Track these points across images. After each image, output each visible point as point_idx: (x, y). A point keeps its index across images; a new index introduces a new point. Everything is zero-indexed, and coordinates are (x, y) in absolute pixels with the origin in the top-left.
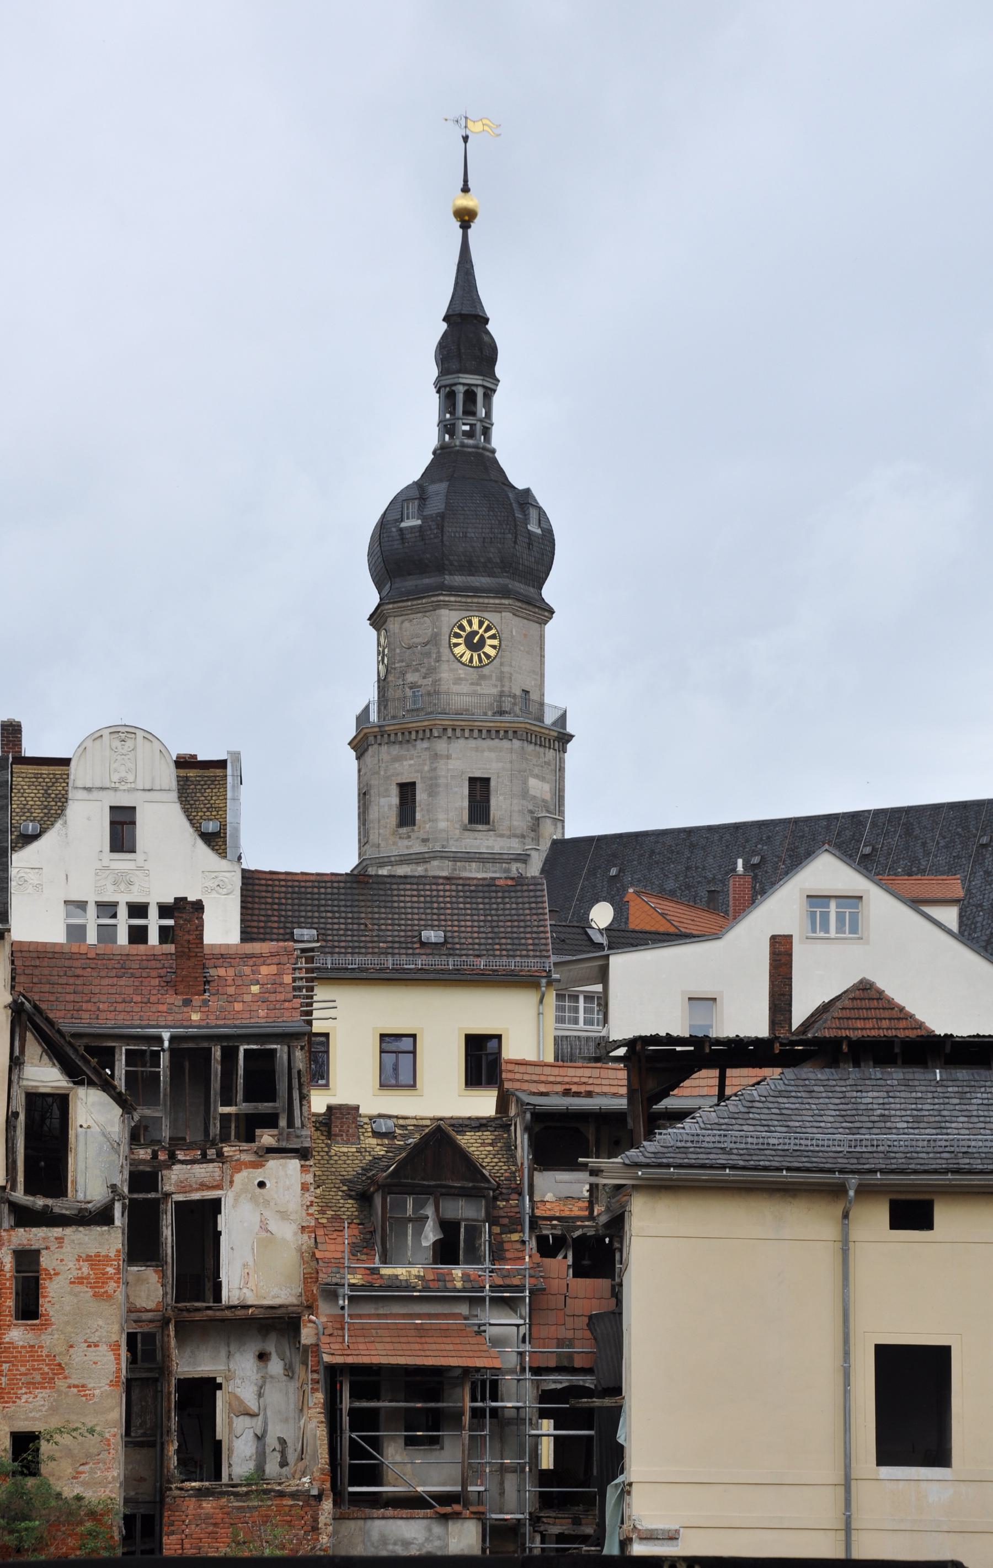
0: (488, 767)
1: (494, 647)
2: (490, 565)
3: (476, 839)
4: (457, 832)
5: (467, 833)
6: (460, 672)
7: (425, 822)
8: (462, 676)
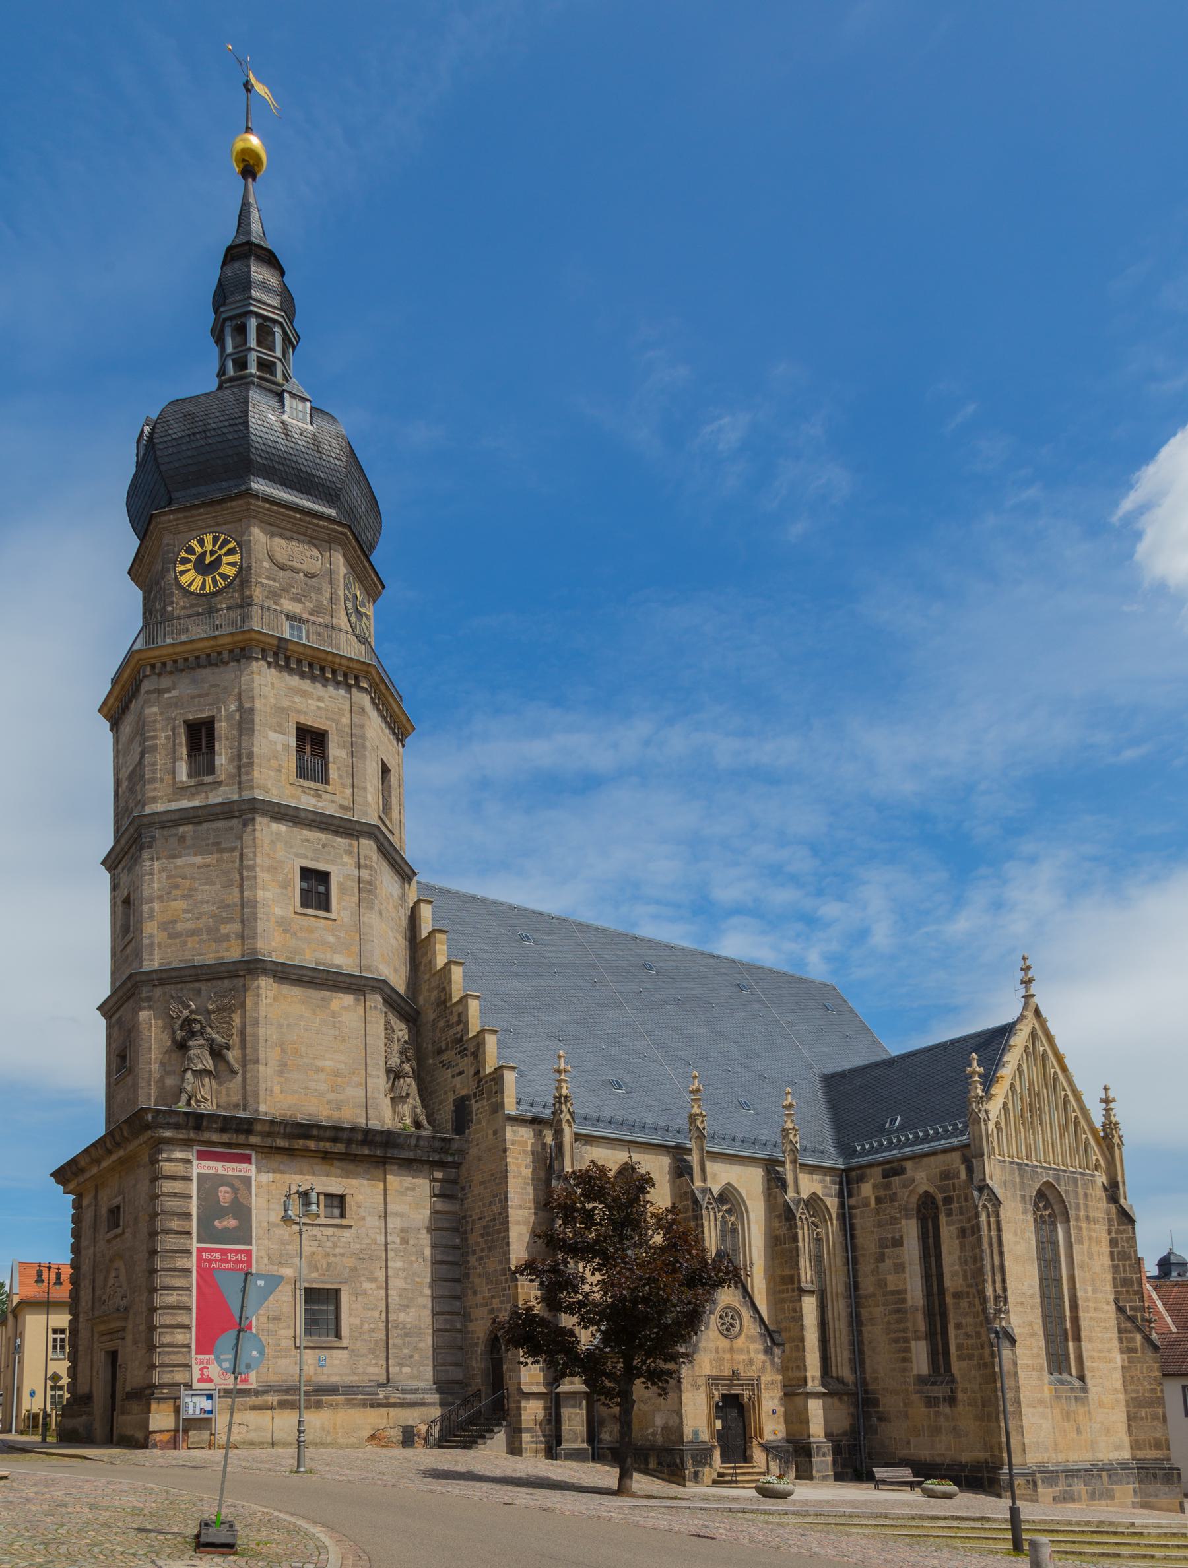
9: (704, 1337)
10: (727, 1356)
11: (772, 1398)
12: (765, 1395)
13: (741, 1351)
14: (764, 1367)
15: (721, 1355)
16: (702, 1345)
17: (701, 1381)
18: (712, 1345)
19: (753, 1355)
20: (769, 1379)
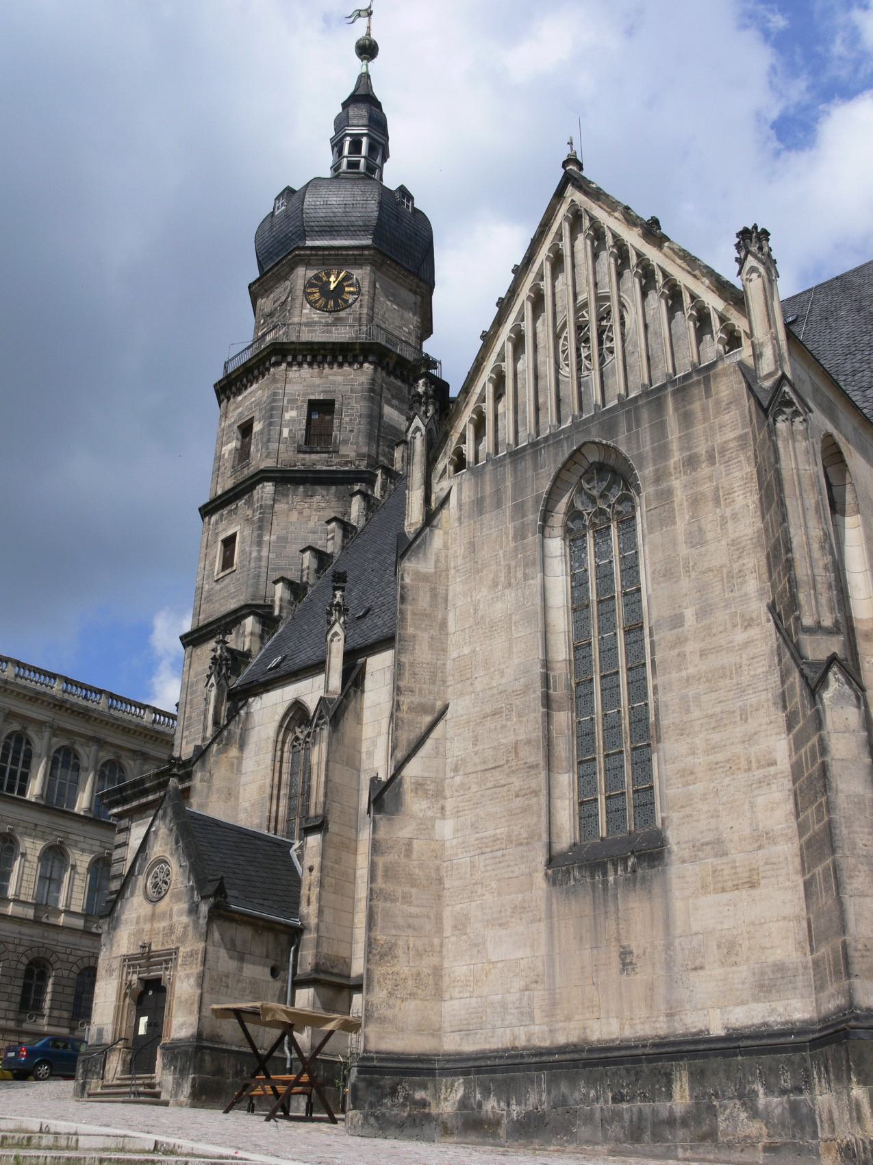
9: (128, 906)
10: (147, 927)
11: (188, 976)
12: (181, 972)
13: (163, 916)
14: (185, 934)
15: (142, 925)
16: (124, 917)
17: (116, 964)
18: (134, 915)
19: (175, 919)
20: (188, 949)
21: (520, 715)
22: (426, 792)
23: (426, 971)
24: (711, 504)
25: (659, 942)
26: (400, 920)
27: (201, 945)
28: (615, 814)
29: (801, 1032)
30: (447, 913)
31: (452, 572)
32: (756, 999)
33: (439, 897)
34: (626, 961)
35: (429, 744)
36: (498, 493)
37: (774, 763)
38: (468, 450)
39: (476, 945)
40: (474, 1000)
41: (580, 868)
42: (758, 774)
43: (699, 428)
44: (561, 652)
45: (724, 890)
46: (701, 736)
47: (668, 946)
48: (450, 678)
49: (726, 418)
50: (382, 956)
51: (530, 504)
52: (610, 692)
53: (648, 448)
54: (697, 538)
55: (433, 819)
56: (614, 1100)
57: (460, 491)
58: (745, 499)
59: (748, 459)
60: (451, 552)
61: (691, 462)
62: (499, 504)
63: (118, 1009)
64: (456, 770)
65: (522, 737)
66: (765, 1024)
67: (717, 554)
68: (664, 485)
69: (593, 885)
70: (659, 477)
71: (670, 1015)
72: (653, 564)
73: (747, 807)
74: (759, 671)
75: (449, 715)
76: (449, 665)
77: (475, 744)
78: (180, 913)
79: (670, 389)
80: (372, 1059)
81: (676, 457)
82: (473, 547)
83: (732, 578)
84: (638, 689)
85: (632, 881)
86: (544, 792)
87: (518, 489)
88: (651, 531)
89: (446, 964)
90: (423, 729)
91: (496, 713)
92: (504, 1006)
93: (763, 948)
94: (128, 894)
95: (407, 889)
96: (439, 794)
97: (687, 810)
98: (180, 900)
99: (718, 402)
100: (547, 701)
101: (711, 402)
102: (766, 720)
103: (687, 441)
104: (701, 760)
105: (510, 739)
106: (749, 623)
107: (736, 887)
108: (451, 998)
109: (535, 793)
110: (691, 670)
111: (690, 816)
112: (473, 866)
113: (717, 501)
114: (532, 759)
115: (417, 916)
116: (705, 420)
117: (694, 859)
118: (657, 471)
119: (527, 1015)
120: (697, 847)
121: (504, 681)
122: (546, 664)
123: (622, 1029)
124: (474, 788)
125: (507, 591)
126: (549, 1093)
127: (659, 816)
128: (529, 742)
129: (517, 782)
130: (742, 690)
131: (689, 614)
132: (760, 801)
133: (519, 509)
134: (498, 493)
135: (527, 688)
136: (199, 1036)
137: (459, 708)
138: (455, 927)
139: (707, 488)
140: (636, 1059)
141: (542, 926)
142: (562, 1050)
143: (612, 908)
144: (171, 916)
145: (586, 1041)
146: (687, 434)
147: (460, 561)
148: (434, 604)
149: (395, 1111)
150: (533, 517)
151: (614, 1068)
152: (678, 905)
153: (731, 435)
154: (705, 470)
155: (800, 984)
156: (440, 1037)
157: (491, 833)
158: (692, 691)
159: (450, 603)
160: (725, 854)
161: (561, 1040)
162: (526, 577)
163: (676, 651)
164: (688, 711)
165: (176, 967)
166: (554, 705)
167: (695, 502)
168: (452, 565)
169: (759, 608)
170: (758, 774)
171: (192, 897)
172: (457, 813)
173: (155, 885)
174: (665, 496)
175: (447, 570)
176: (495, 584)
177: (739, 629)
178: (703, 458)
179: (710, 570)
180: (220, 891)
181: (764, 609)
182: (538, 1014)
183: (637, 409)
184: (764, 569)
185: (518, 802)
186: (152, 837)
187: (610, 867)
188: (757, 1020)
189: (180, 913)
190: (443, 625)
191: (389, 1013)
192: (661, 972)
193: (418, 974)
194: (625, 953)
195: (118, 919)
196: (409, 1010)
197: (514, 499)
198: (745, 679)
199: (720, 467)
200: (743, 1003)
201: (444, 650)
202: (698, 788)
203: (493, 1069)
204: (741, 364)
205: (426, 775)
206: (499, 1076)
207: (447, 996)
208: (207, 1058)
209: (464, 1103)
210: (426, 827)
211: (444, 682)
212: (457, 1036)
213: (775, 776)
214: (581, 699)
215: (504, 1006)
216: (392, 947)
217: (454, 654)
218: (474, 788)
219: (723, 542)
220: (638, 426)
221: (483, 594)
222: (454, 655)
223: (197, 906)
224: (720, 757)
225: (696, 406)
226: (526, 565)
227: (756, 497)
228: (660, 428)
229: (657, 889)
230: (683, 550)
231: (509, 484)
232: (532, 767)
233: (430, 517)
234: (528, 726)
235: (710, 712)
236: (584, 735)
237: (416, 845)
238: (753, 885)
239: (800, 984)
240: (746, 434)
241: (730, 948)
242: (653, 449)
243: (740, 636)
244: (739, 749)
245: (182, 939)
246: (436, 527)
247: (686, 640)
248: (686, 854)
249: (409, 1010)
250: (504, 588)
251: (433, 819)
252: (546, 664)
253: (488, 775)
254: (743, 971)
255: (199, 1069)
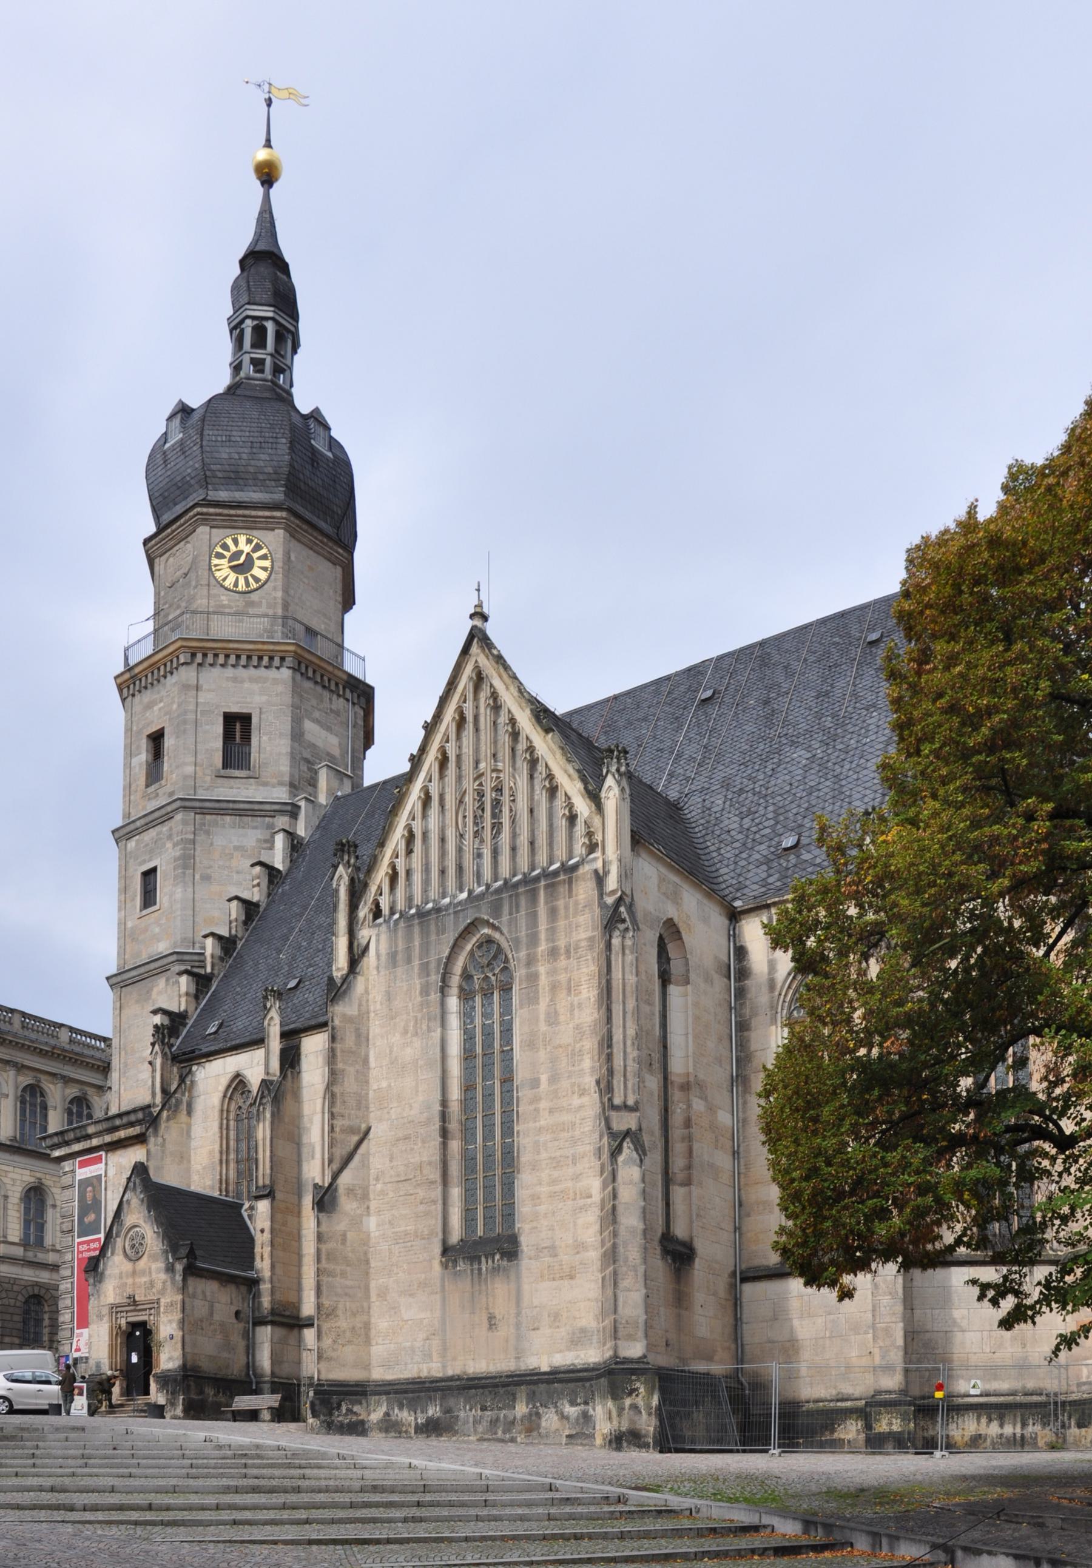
0: (248, 700)
1: (265, 569)
2: (261, 477)
3: (231, 788)
4: (208, 778)
5: (220, 780)
6: (223, 598)
7: (172, 772)
8: (226, 602)
9: (110, 1263)
10: (130, 1281)
11: (170, 1322)
12: (163, 1318)
13: (143, 1273)
14: (164, 1288)
15: (124, 1280)
16: (107, 1273)
17: (105, 1311)
18: (117, 1271)
19: (154, 1275)
20: (169, 1300)
21: (424, 1142)
22: (355, 1195)
23: (359, 1325)
24: (565, 992)
25: (513, 1311)
26: (339, 1291)
27: (180, 1297)
28: (489, 1219)
29: (593, 1369)
30: (373, 1284)
31: (372, 1015)
32: (569, 1349)
33: (367, 1273)
34: (492, 1323)
35: (357, 1158)
36: (408, 949)
37: (590, 1196)
38: (385, 904)
39: (394, 1308)
40: (392, 1346)
41: (464, 1258)
42: (581, 1202)
43: (561, 923)
44: (455, 1093)
45: (554, 1279)
46: (547, 1171)
47: (518, 1314)
48: (371, 1106)
49: (581, 919)
50: (328, 1315)
51: (433, 966)
52: (489, 1135)
53: (523, 933)
54: (553, 1019)
55: (361, 1216)
56: (482, 1409)
57: (378, 941)
58: (589, 993)
59: (593, 958)
60: (371, 997)
61: (553, 953)
62: (409, 960)
63: (112, 1347)
64: (377, 1179)
65: (425, 1159)
66: (573, 1364)
67: (565, 1034)
68: (533, 969)
69: (472, 1270)
70: (531, 961)
71: (518, 1358)
72: (522, 1034)
73: (571, 1225)
74: (587, 1129)
75: (371, 1135)
76: (371, 1093)
77: (391, 1161)
78: (158, 1271)
79: (543, 883)
80: (323, 1385)
81: (543, 947)
82: (389, 996)
83: (575, 1056)
84: (508, 1130)
85: (496, 1270)
86: (440, 1202)
87: (425, 948)
88: (521, 1008)
89: (373, 1320)
90: (352, 1147)
91: (406, 1138)
92: (413, 1349)
93: (575, 1318)
94: (109, 1254)
95: (343, 1267)
96: (365, 1197)
97: (534, 1224)
98: (157, 1260)
99: (576, 903)
100: (444, 1133)
101: (572, 901)
102: (587, 1165)
103: (552, 931)
104: (544, 1189)
105: (415, 1159)
106: (583, 1093)
107: (562, 1278)
108: (377, 1344)
109: (434, 1202)
110: (543, 1123)
111: (536, 1228)
112: (390, 1253)
113: (569, 990)
114: (432, 1177)
115: (351, 1287)
116: (567, 917)
117: (537, 1257)
118: (529, 955)
119: (427, 1356)
120: (539, 1250)
121: (412, 1113)
122: (444, 1103)
123: (488, 1366)
124: (391, 1194)
125: (415, 1039)
126: (441, 1406)
127: (517, 1225)
128: (430, 1163)
129: (421, 1193)
130: (574, 1142)
131: (544, 1078)
132: (580, 1222)
133: (425, 969)
134: (408, 949)
135: (429, 1121)
136: (184, 1367)
137: (380, 1131)
138: (378, 1295)
139: (563, 977)
140: (496, 1386)
141: (438, 1297)
142: (451, 1379)
143: (484, 1287)
144: (150, 1273)
145: (465, 1373)
146: (552, 928)
147: (378, 1007)
148: (358, 1043)
149: (340, 1419)
150: (435, 978)
151: (481, 1391)
152: (526, 1287)
153: (583, 935)
154: (563, 962)
155: (594, 1341)
156: (369, 1370)
157: (403, 1229)
158: (542, 1139)
159: (371, 1042)
160: (556, 1256)
161: (450, 1373)
162: (429, 1030)
163: (532, 1108)
164: (538, 1153)
165: (158, 1314)
166: (450, 1136)
167: (554, 987)
168: (372, 1008)
169: (589, 1081)
170: (581, 1202)
171: (167, 1259)
172: (379, 1212)
173: (133, 1246)
174: (533, 978)
175: (368, 1013)
176: (406, 1032)
177: (576, 1096)
178: (562, 951)
179: (560, 1046)
180: (191, 1255)
181: (594, 1083)
182: (435, 1356)
183: (517, 895)
184: (596, 1052)
185: (422, 1208)
186: (125, 1206)
187: (483, 1259)
188: (568, 1362)
189: (158, 1271)
190: (366, 1061)
191: (334, 1355)
192: (512, 1330)
193: (354, 1328)
194: (491, 1318)
195: (102, 1274)
196: (348, 1352)
197: (421, 959)
198: (577, 1133)
199: (573, 962)
200: (561, 1351)
201: (367, 1082)
202: (542, 1209)
203: (406, 1392)
204: (596, 871)
205: (356, 1182)
206: (411, 1395)
207: (373, 1342)
208: (192, 1383)
209: (387, 1414)
210: (357, 1222)
211: (367, 1108)
212: (381, 1370)
213: (590, 1206)
214: (468, 1134)
215: (413, 1351)
216: (334, 1309)
217: (375, 1087)
218: (391, 1194)
219: (571, 1026)
220: (518, 912)
221: (396, 1038)
222: (375, 1087)
223: (173, 1265)
224: (557, 1188)
225: (561, 903)
226: (429, 1020)
227: (596, 992)
228: (533, 916)
229: (513, 1277)
230: (543, 1027)
231: (417, 943)
232: (432, 1183)
233: (355, 960)
234: (430, 1151)
235: (553, 1155)
236: (468, 1160)
237: (350, 1235)
238: (572, 1277)
239: (594, 1341)
240: (594, 937)
241: (556, 1316)
242: (527, 935)
243: (576, 1101)
244: (570, 1184)
245: (162, 1292)
246: (358, 973)
247: (540, 1099)
248: (532, 1253)
249: (348, 1352)
250: (413, 1036)
251: (361, 1216)
252: (444, 1103)
253: (400, 1185)
254: (563, 1332)
255: (186, 1391)
